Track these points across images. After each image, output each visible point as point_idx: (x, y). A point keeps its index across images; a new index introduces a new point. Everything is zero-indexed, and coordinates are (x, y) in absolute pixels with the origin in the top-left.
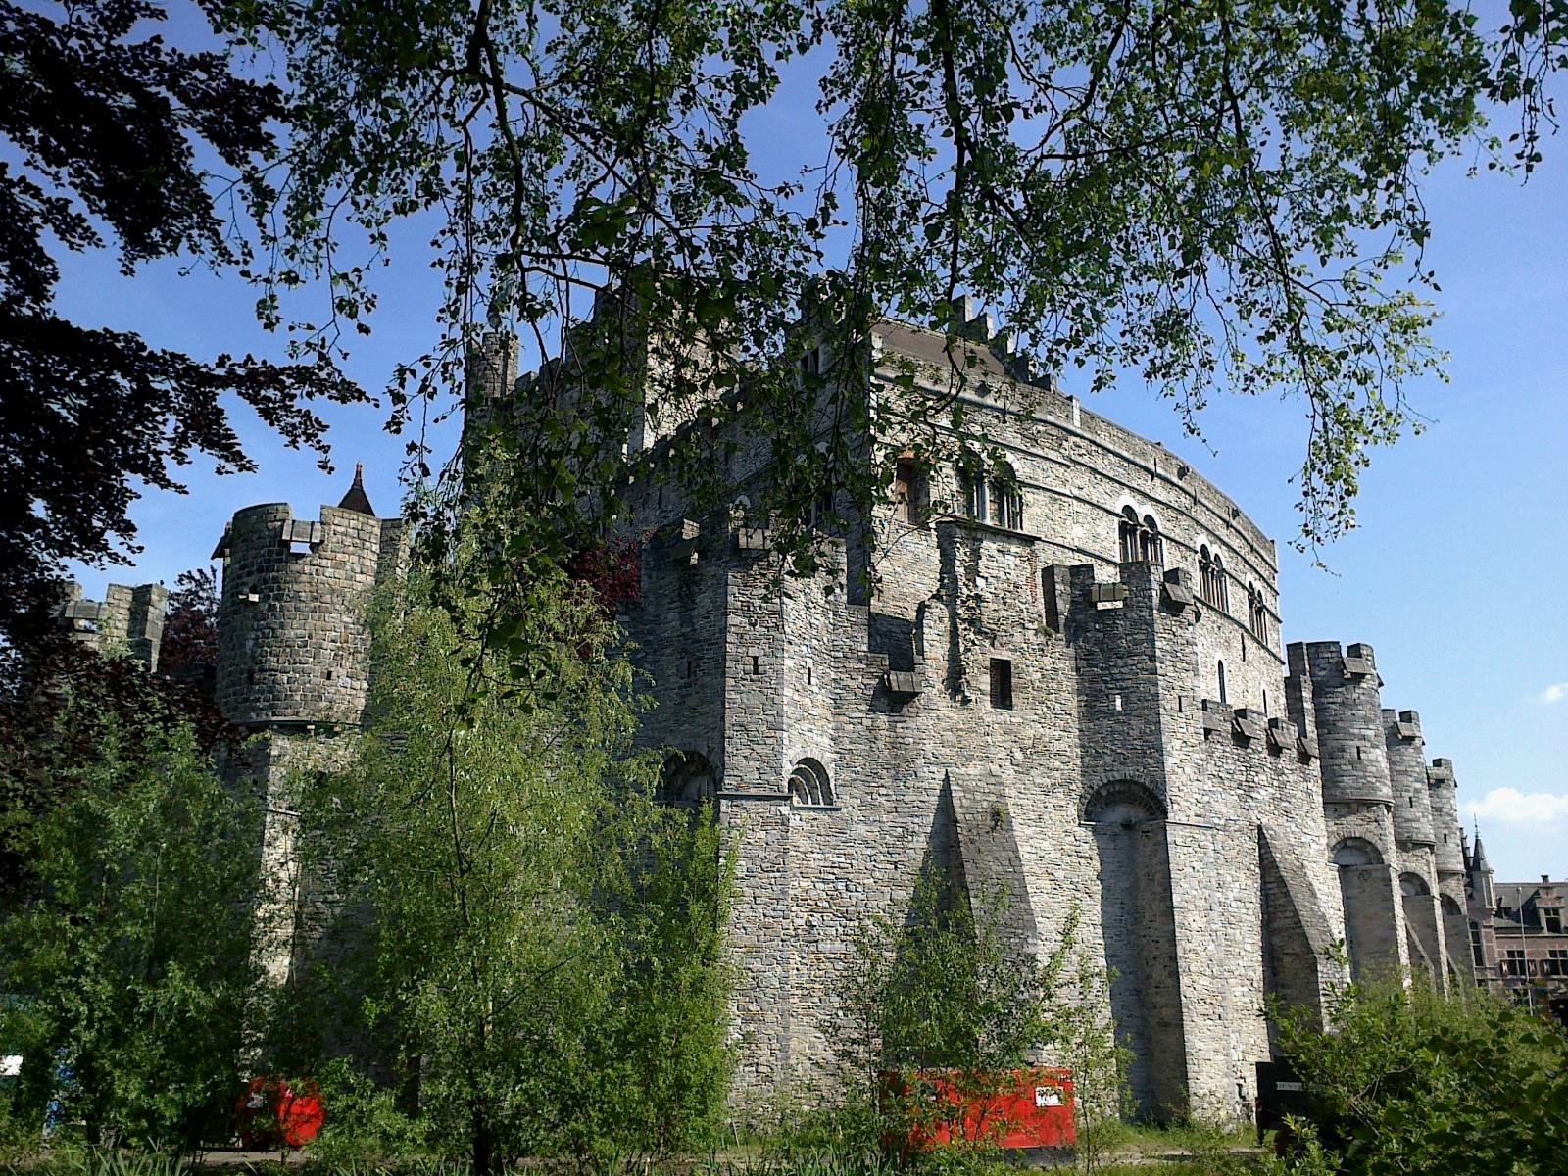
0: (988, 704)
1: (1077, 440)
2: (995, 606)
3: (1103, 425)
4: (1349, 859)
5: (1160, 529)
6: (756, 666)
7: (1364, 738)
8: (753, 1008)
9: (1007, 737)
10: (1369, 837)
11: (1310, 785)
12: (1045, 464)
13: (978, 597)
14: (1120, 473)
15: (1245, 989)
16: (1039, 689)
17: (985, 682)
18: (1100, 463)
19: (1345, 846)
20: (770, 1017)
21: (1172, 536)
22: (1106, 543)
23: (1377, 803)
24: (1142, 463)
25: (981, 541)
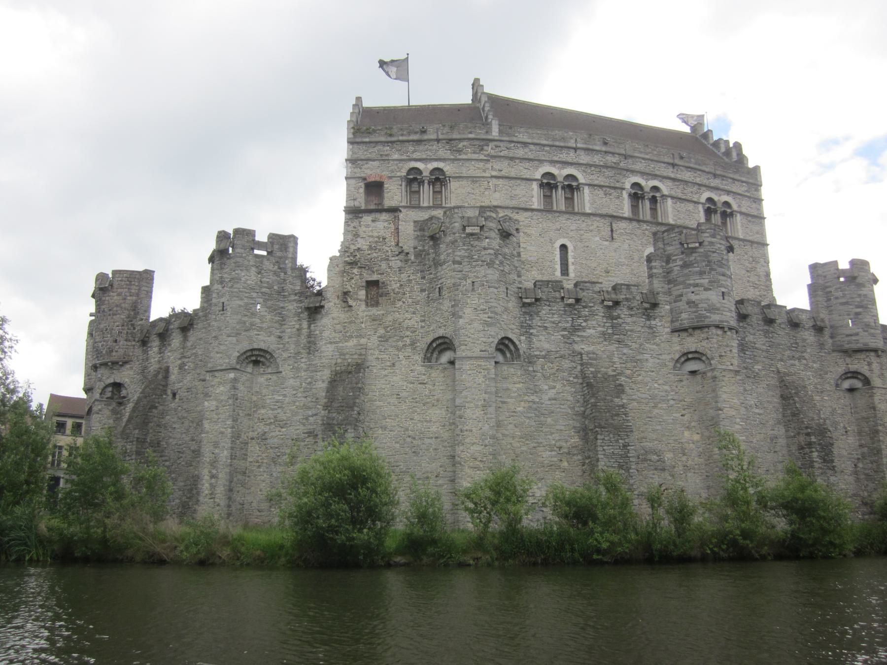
0: (363, 307)
1: (496, 143)
2: (369, 252)
5: (582, 179)
6: (223, 307)
7: (697, 285)
8: (214, 472)
9: (375, 322)
10: (700, 350)
11: (653, 322)
14: (542, 155)
15: (554, 453)
16: (398, 293)
17: (362, 294)
18: (520, 152)
19: (688, 360)
20: (221, 476)
21: (596, 182)
23: (708, 327)
24: (562, 144)
25: (361, 218)
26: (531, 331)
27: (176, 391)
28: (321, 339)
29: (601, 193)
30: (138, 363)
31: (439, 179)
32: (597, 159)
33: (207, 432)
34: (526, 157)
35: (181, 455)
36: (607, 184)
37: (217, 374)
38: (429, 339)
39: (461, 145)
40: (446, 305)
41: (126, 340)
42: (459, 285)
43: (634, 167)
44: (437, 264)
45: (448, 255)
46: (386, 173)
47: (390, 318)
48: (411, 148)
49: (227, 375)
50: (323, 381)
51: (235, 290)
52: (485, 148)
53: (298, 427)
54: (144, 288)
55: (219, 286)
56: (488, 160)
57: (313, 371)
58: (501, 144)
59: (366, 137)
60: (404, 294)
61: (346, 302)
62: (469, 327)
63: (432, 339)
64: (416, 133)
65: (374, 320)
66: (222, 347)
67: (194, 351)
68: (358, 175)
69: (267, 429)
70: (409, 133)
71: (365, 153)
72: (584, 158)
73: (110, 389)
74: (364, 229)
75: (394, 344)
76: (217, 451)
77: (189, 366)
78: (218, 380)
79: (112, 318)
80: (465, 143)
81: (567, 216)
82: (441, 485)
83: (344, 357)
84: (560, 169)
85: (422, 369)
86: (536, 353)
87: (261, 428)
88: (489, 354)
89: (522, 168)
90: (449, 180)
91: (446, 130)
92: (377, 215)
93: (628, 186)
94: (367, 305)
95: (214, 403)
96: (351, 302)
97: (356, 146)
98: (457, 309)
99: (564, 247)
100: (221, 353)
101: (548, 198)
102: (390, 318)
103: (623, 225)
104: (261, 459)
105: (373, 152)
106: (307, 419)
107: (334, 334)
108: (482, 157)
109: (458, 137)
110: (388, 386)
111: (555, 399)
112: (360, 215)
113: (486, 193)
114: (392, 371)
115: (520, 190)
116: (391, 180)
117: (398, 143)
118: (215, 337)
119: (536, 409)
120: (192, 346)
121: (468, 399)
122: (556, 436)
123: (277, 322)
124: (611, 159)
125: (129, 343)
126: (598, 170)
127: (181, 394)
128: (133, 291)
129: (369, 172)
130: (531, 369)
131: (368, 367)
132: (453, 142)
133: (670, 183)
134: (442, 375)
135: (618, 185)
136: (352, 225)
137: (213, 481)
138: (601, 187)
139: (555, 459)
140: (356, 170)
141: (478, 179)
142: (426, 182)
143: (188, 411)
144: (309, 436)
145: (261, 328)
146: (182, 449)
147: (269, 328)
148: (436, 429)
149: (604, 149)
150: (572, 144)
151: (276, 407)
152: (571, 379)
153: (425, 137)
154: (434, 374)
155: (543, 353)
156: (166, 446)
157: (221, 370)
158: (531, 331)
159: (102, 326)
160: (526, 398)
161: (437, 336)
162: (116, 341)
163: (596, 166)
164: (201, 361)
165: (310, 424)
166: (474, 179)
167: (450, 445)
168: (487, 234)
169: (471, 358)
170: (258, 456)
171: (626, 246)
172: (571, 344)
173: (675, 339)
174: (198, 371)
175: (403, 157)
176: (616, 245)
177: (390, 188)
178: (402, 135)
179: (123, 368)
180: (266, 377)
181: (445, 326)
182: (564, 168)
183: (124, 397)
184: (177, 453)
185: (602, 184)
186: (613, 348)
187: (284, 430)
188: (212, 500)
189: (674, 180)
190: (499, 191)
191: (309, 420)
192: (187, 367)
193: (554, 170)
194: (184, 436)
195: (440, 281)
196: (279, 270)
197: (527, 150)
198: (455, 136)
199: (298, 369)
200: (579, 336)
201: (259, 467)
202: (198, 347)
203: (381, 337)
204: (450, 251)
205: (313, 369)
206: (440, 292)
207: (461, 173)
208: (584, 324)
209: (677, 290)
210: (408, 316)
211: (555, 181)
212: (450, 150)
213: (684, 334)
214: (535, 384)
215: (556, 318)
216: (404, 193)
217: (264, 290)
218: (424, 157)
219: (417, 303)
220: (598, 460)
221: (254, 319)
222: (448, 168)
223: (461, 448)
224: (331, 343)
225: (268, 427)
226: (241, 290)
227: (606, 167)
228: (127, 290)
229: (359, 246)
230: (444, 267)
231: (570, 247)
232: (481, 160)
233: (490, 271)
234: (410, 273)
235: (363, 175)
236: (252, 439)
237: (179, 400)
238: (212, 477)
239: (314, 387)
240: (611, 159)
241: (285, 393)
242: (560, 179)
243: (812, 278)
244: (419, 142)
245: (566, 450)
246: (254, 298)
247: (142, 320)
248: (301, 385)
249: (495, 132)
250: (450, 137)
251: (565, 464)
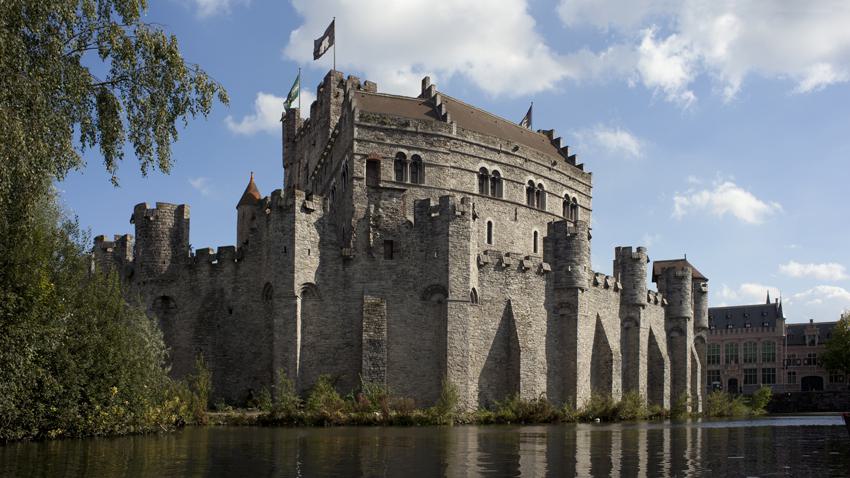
0: (383, 259)
4: (561, 312)
13: (379, 216)
18: (468, 150)
23: (577, 288)
29: (511, 185)
31: (417, 164)
32: (511, 161)
38: (425, 285)
40: (441, 264)
44: (434, 234)
46: (381, 154)
47: (400, 268)
72: (504, 159)
85: (419, 304)
94: (385, 258)
96: (374, 255)
99: (490, 223)
101: (481, 185)
102: (400, 268)
103: (521, 210)
105: (369, 135)
115: (467, 177)
124: (519, 161)
133: (547, 181)
138: (513, 181)
153: (409, 129)
173: (556, 294)
175: (394, 143)
186: (526, 298)
189: (550, 180)
198: (429, 131)
209: (560, 263)
213: (562, 291)
219: (417, 259)
222: (423, 156)
231: (494, 225)
242: (490, 173)
243: (617, 256)
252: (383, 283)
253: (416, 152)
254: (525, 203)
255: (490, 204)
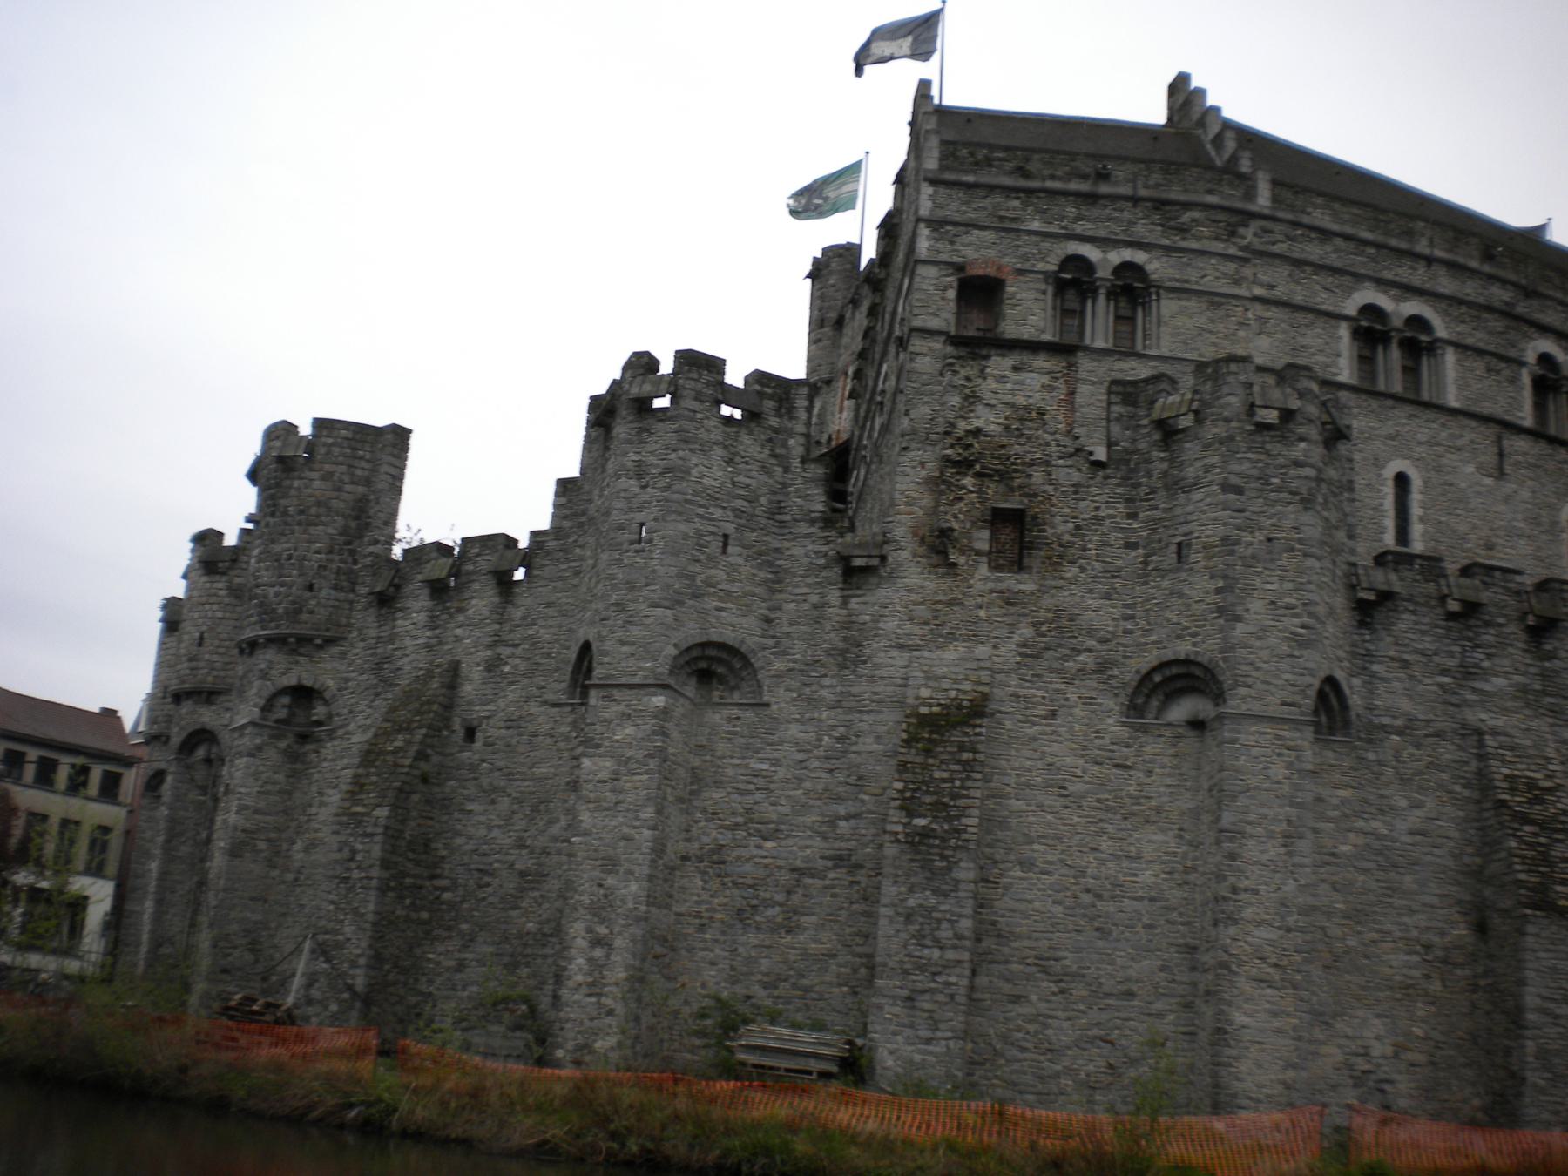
0: (983, 569)
2: (1005, 441)
3: (1320, 201)
5: (1441, 331)
8: (602, 930)
9: (1012, 609)
12: (1200, 262)
14: (1360, 263)
15: (1415, 958)
17: (982, 539)
18: (1314, 251)
20: (618, 942)
21: (1470, 341)
22: (1320, 358)
24: (1404, 245)
25: (987, 357)
26: (1375, 667)
27: (475, 723)
28: (875, 635)
29: (1479, 365)
30: (362, 644)
32: (1470, 289)
33: (586, 833)
34: (1327, 262)
35: (487, 879)
36: (1491, 348)
37: (617, 694)
39: (1187, 217)
40: (1200, 586)
41: (335, 588)
42: (1238, 543)
43: (1537, 316)
44: (1176, 486)
45: (1208, 469)
47: (1047, 602)
48: (1071, 211)
49: (645, 699)
50: (878, 738)
51: (676, 496)
52: (1242, 231)
53: (808, 843)
54: (385, 468)
55: (632, 482)
56: (1245, 260)
57: (851, 710)
58: (1277, 227)
59: (967, 172)
60: (1084, 549)
61: (943, 553)
62: (1258, 643)
63: (1155, 663)
64: (1084, 177)
65: (1008, 603)
66: (636, 632)
67: (531, 632)
68: (944, 257)
69: (725, 838)
70: (1068, 177)
71: (964, 208)
72: (1446, 284)
73: (286, 700)
74: (994, 385)
75: (1056, 665)
76: (610, 881)
77: (515, 667)
78: (621, 708)
79: (305, 532)
80: (1196, 214)
81: (1409, 409)
82: (1160, 1015)
83: (936, 685)
84: (1397, 299)
85: (1123, 733)
86: (1386, 721)
87: (711, 835)
88: (1302, 714)
89: (1318, 287)
90: (1158, 295)
91: (1156, 177)
92: (1026, 358)
93: (1531, 357)
95: (608, 764)
96: (954, 556)
97: (942, 190)
98: (1231, 599)
99: (1401, 480)
100: (633, 644)
101: (1366, 361)
103: (1520, 444)
104: (707, 910)
106: (832, 823)
107: (908, 628)
108: (1232, 251)
109: (1183, 198)
110: (1040, 764)
111: (1422, 833)
112: (984, 352)
113: (1241, 333)
114: (1048, 729)
116: (1021, 278)
117: (1042, 195)
118: (617, 604)
119: (1380, 853)
120: (524, 618)
121: (1252, 817)
122: (1421, 919)
123: (764, 582)
124: (1500, 295)
125: (342, 596)
126: (1474, 313)
127: (491, 730)
128: (359, 472)
129: (970, 253)
130: (1371, 756)
131: (992, 715)
132: (1168, 208)
134: (1171, 751)
135: (1512, 353)
136: (963, 372)
137: (598, 952)
138: (1480, 352)
139: (1416, 973)
140: (940, 245)
141: (1223, 300)
142: (1102, 291)
143: (510, 776)
144: (836, 867)
145: (728, 593)
146: (491, 864)
147: (745, 595)
148: (1153, 879)
149: (1487, 268)
150: (1422, 247)
151: (751, 787)
152: (1458, 788)
153: (1104, 189)
154: (1153, 747)
155: (1399, 722)
156: (444, 853)
157: (630, 686)
158: (1375, 667)
159: (277, 548)
160: (1360, 824)
161: (1169, 655)
162: (310, 588)
163: (1470, 304)
164: (548, 656)
165: (841, 837)
166: (1214, 299)
167: (1185, 919)
168: (1302, 431)
169: (1259, 718)
170: (698, 903)
171: (1525, 494)
172: (1457, 706)
174: (539, 680)
175: (1054, 229)
176: (1509, 487)
177: (1019, 297)
178: (1053, 177)
179: (324, 655)
180: (726, 712)
181: (1194, 635)
182: (1405, 300)
183: (319, 723)
184: (477, 875)
185: (1481, 345)
186: (1542, 724)
187: (769, 844)
188: (593, 1000)
190: (1269, 334)
191: (836, 826)
192: (507, 669)
193: (1384, 302)
194: (496, 833)
195: (1184, 529)
196: (773, 461)
197: (1329, 248)
198: (1175, 194)
199: (813, 702)
200: (1474, 690)
201: (702, 928)
202: (541, 622)
203: (1024, 645)
204: (1215, 460)
205: (854, 704)
206: (1179, 554)
207: (1186, 281)
208: (1486, 664)
210: (1095, 603)
211: (1384, 324)
212: (1162, 225)
214: (1382, 792)
215: (1428, 643)
216: (1050, 312)
217: (739, 503)
218: (1102, 233)
219: (1115, 573)
220: (1522, 982)
221: (713, 572)
222: (1156, 266)
223: (1232, 930)
224: (901, 647)
225: (729, 834)
226: (689, 497)
227: (1489, 309)
228: (344, 468)
229: (979, 423)
230: (1196, 496)
231: (1416, 482)
232: (1232, 258)
233: (1307, 518)
234: (1102, 499)
235: (956, 259)
236: (685, 858)
237: (486, 744)
238: (597, 942)
239: (854, 748)
240: (1500, 295)
241: (775, 755)
244: (1091, 198)
245: (1440, 953)
246: (714, 520)
247: (376, 542)
248: (820, 740)
249: (1263, 199)
250: (1164, 196)
251: (1436, 986)
252: (982, 650)
253: (1127, 255)
254: (1528, 422)
255: (1400, 420)
